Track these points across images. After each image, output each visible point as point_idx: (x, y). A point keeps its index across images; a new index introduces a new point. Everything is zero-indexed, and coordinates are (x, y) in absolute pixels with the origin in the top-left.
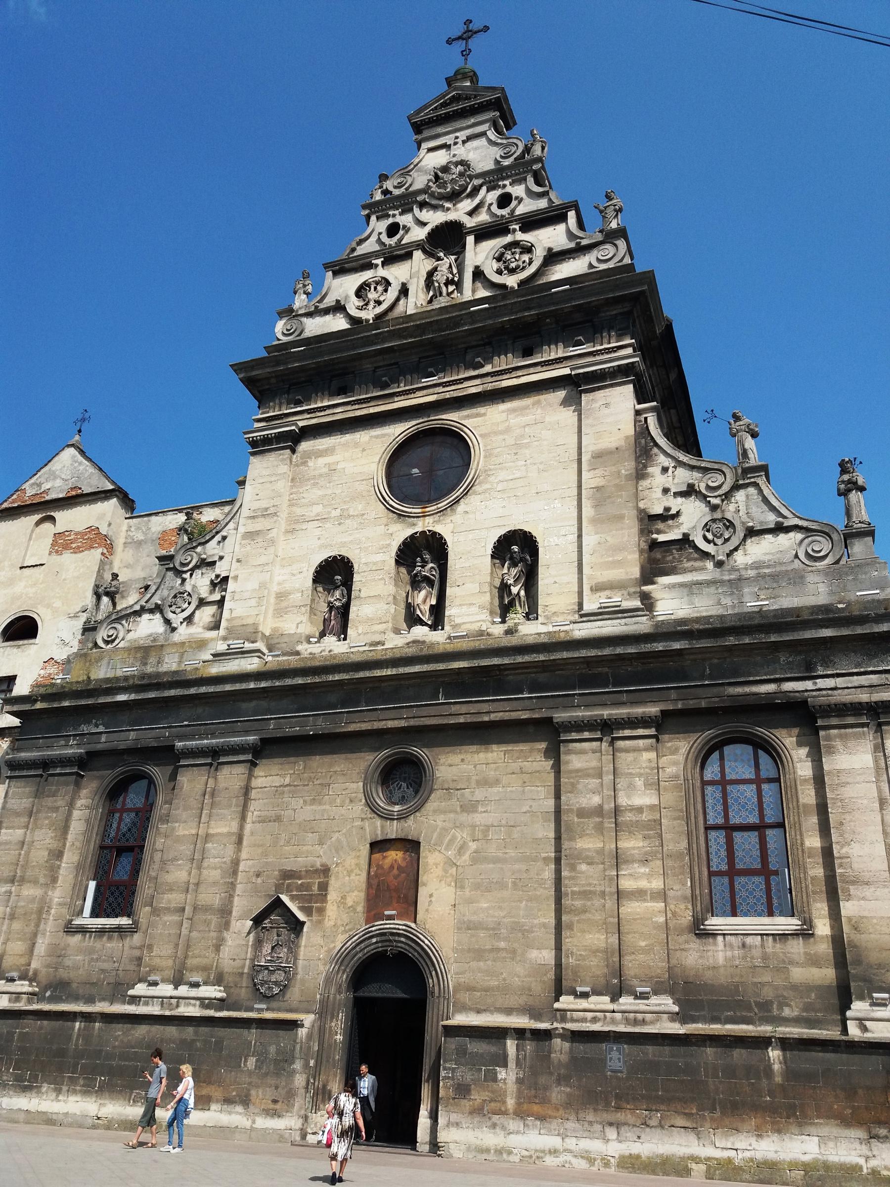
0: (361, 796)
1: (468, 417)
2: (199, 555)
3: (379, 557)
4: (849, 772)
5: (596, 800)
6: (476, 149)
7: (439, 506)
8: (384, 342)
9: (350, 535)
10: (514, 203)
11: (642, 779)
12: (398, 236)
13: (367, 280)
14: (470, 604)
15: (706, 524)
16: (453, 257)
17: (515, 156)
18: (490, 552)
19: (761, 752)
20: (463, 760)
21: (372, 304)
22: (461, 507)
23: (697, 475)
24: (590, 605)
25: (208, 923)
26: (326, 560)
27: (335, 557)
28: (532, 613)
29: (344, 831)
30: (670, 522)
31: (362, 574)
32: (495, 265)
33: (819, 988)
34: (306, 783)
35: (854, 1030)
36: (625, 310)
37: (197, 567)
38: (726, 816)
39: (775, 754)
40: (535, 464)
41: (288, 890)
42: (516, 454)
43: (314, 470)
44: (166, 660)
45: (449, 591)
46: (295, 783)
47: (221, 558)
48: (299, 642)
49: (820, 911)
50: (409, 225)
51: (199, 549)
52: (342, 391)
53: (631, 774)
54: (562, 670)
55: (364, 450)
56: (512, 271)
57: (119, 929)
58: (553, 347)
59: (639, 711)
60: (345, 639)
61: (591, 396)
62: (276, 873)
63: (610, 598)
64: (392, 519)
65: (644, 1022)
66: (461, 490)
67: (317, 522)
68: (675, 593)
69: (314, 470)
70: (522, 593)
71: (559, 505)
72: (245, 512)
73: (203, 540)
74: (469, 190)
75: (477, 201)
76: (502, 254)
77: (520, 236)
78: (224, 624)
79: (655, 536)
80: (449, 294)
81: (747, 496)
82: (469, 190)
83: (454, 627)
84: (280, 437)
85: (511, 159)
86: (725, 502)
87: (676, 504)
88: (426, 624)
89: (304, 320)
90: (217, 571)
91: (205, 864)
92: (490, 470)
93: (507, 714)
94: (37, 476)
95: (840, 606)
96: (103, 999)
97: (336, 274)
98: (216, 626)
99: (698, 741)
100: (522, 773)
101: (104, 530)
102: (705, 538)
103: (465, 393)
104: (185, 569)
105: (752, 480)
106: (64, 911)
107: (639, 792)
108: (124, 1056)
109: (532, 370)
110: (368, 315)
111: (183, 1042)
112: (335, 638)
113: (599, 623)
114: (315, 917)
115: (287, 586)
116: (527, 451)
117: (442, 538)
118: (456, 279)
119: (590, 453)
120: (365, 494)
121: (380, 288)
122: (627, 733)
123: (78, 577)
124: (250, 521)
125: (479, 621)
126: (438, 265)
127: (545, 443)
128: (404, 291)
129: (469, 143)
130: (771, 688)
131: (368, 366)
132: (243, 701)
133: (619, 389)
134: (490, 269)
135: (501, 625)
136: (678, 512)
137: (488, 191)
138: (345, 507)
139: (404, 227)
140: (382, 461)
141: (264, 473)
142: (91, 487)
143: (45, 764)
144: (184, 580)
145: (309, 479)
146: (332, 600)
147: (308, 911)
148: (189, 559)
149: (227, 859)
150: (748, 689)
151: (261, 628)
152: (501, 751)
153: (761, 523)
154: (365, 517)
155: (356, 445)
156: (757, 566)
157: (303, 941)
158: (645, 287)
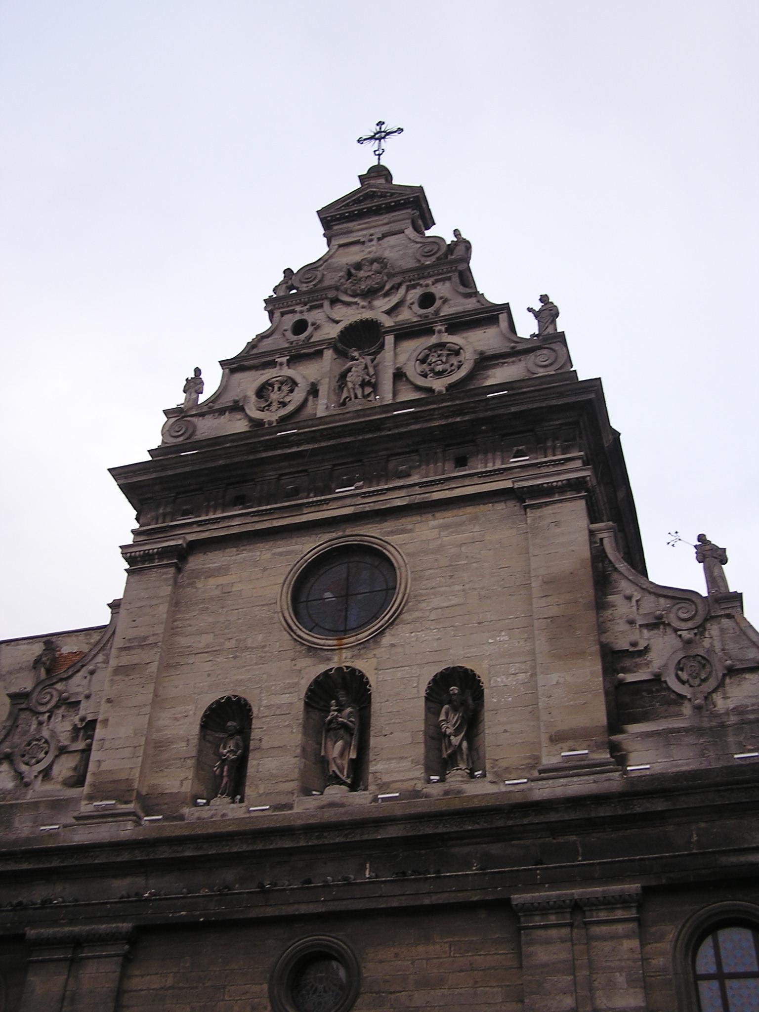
0: (266, 1002)
1: (392, 533)
2: (60, 693)
3: (285, 699)
6: (393, 247)
7: (359, 637)
8: (290, 447)
10: (438, 303)
11: (624, 974)
12: (306, 334)
13: (269, 380)
14: (402, 758)
15: (679, 662)
16: (369, 358)
17: (437, 255)
18: (423, 694)
20: (397, 955)
21: (275, 405)
22: (386, 640)
24: (549, 759)
26: (218, 702)
27: (229, 698)
30: (638, 660)
31: (264, 719)
32: (420, 368)
34: (195, 985)
36: (570, 420)
37: (57, 707)
40: (475, 589)
42: (451, 577)
44: (17, 824)
45: (373, 742)
46: (181, 985)
47: (88, 697)
48: (184, 803)
50: (318, 322)
51: (59, 686)
52: (240, 500)
53: (610, 967)
54: (519, 839)
55: (265, 569)
56: (440, 374)
59: (615, 888)
60: (242, 801)
61: (538, 513)
64: (300, 652)
66: (386, 618)
67: (206, 655)
70: (465, 744)
71: (506, 638)
72: (118, 642)
73: (65, 676)
74: (387, 287)
75: (394, 300)
76: (427, 356)
77: (447, 338)
78: (89, 779)
79: (621, 675)
80: (365, 397)
81: (722, 631)
82: (387, 287)
83: (384, 787)
84: (164, 553)
85: (433, 258)
86: (698, 637)
87: (644, 638)
88: (344, 783)
90: (82, 713)
92: (421, 595)
93: (453, 895)
97: (233, 371)
98: (78, 780)
99: (688, 925)
100: (472, 970)
102: (678, 678)
103: (388, 506)
104: (42, 709)
105: (727, 612)
107: (621, 991)
109: (467, 482)
110: (272, 416)
112: (228, 799)
113: (562, 780)
118: (373, 381)
119: (540, 578)
121: (285, 388)
122: (603, 915)
124: (124, 653)
125: (412, 779)
126: (352, 365)
127: (486, 565)
128: (314, 391)
129: (386, 239)
131: (272, 475)
132: (115, 877)
133: (568, 504)
134: (413, 371)
135: (440, 784)
136: (646, 648)
137: (407, 290)
140: (287, 582)
144: (40, 723)
145: (196, 603)
148: (48, 697)
150: (743, 859)
151: (136, 785)
152: (446, 943)
153: (741, 660)
154: (266, 649)
156: (739, 711)
158: (593, 396)
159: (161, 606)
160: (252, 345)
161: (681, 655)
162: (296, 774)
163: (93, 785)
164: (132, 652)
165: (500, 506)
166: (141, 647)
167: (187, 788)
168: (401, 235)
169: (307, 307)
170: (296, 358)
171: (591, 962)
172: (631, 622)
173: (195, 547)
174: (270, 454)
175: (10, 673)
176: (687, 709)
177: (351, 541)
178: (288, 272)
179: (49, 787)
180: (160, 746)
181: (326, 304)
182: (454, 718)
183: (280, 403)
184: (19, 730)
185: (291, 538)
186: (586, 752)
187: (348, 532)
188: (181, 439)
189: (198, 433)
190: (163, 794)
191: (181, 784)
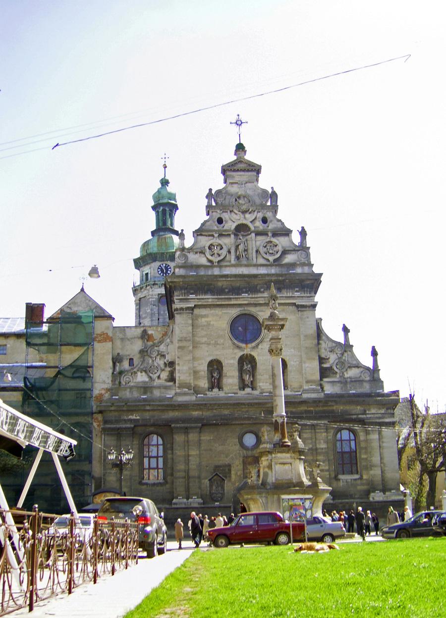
0: (238, 443)
1: (259, 311)
2: (158, 351)
3: (232, 361)
4: (373, 439)
6: (250, 189)
8: (228, 278)
12: (222, 225)
14: (266, 382)
19: (351, 433)
22: (260, 347)
23: (334, 345)
24: (306, 387)
26: (212, 361)
29: (234, 454)
30: (328, 361)
35: (371, 499)
37: (158, 355)
38: (342, 450)
45: (258, 377)
47: (168, 354)
48: (206, 391)
51: (156, 348)
55: (220, 318)
58: (288, 290)
61: (302, 313)
62: (213, 466)
63: (311, 385)
68: (329, 384)
69: (201, 323)
74: (250, 210)
82: (250, 210)
83: (262, 390)
84: (187, 308)
89: (187, 254)
91: (190, 464)
95: (373, 394)
101: (110, 334)
106: (138, 478)
112: (218, 390)
115: (198, 368)
117: (254, 357)
124: (180, 342)
128: (229, 252)
129: (247, 184)
132: (193, 411)
134: (262, 250)
138: (216, 340)
141: (183, 322)
142: (98, 313)
144: (153, 361)
146: (215, 375)
147: (226, 477)
149: (197, 462)
151: (192, 385)
153: (352, 364)
155: (217, 315)
156: (350, 378)
159: (190, 327)
160: (203, 224)
161: (337, 361)
162: (238, 384)
163: (179, 384)
165: (291, 307)
166: (186, 341)
167: (206, 386)
168: (252, 184)
169: (222, 212)
170: (221, 235)
171: (316, 438)
172: (326, 350)
173: (196, 306)
174: (221, 279)
175: (132, 339)
176: (338, 376)
177: (246, 312)
178: (210, 190)
179: (160, 381)
180: (196, 373)
181: (229, 212)
185: (227, 307)
186: (315, 387)
187: (246, 309)
190: (199, 387)
191: (204, 385)
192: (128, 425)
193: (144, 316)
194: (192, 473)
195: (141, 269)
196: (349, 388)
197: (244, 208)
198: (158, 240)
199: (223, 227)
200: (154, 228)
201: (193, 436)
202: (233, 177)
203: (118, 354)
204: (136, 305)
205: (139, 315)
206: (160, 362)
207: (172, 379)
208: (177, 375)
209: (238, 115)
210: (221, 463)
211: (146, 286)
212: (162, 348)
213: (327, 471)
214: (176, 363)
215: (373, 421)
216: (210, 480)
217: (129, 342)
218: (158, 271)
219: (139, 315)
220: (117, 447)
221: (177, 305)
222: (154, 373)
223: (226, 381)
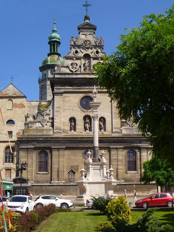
3: (80, 118)
5: (115, 158)
6: (91, 37)
8: (79, 79)
9: (75, 113)
10: (99, 53)
12: (78, 54)
21: (74, 68)
25: (62, 173)
26: (71, 117)
28: (105, 130)
33: (138, 179)
37: (46, 115)
39: (135, 152)
41: (73, 168)
43: (66, 100)
49: (139, 170)
51: (45, 111)
52: (71, 86)
55: (75, 98)
57: (46, 174)
65: (121, 183)
75: (92, 51)
89: (61, 68)
91: (60, 165)
94: (5, 90)
96: (45, 183)
108: (52, 190)
111: (61, 188)
114: (77, 172)
115: (65, 121)
116: (103, 103)
120: (77, 106)
122: (119, 149)
123: (21, 113)
124: (56, 109)
130: (136, 145)
138: (73, 108)
139: (79, 52)
143: (27, 149)
144: (44, 117)
147: (76, 171)
157: (76, 175)
163: (55, 128)
164: (58, 108)
166: (59, 108)
167: (69, 129)
175: (34, 106)
179: (47, 127)
182: (102, 123)
183: (75, 68)
184: (40, 117)
188: (59, 71)
189: (61, 70)
192: (32, 147)
193: (43, 94)
194: (60, 169)
195: (42, 72)
196: (134, 131)
197: (87, 47)
198: (51, 59)
199: (78, 55)
200: (49, 52)
201: (61, 152)
202: (83, 32)
203: (28, 114)
204: (40, 88)
205: (41, 93)
206: (47, 118)
207: (53, 126)
208: (55, 124)
209: (86, 2)
210: (74, 165)
211: (45, 80)
212: (48, 112)
213: (122, 169)
214: (54, 118)
215: (145, 147)
216: (68, 173)
217: (33, 108)
218: (50, 73)
219: (41, 93)
220: (26, 157)
221: (56, 91)
222: (44, 123)
223: (77, 127)
